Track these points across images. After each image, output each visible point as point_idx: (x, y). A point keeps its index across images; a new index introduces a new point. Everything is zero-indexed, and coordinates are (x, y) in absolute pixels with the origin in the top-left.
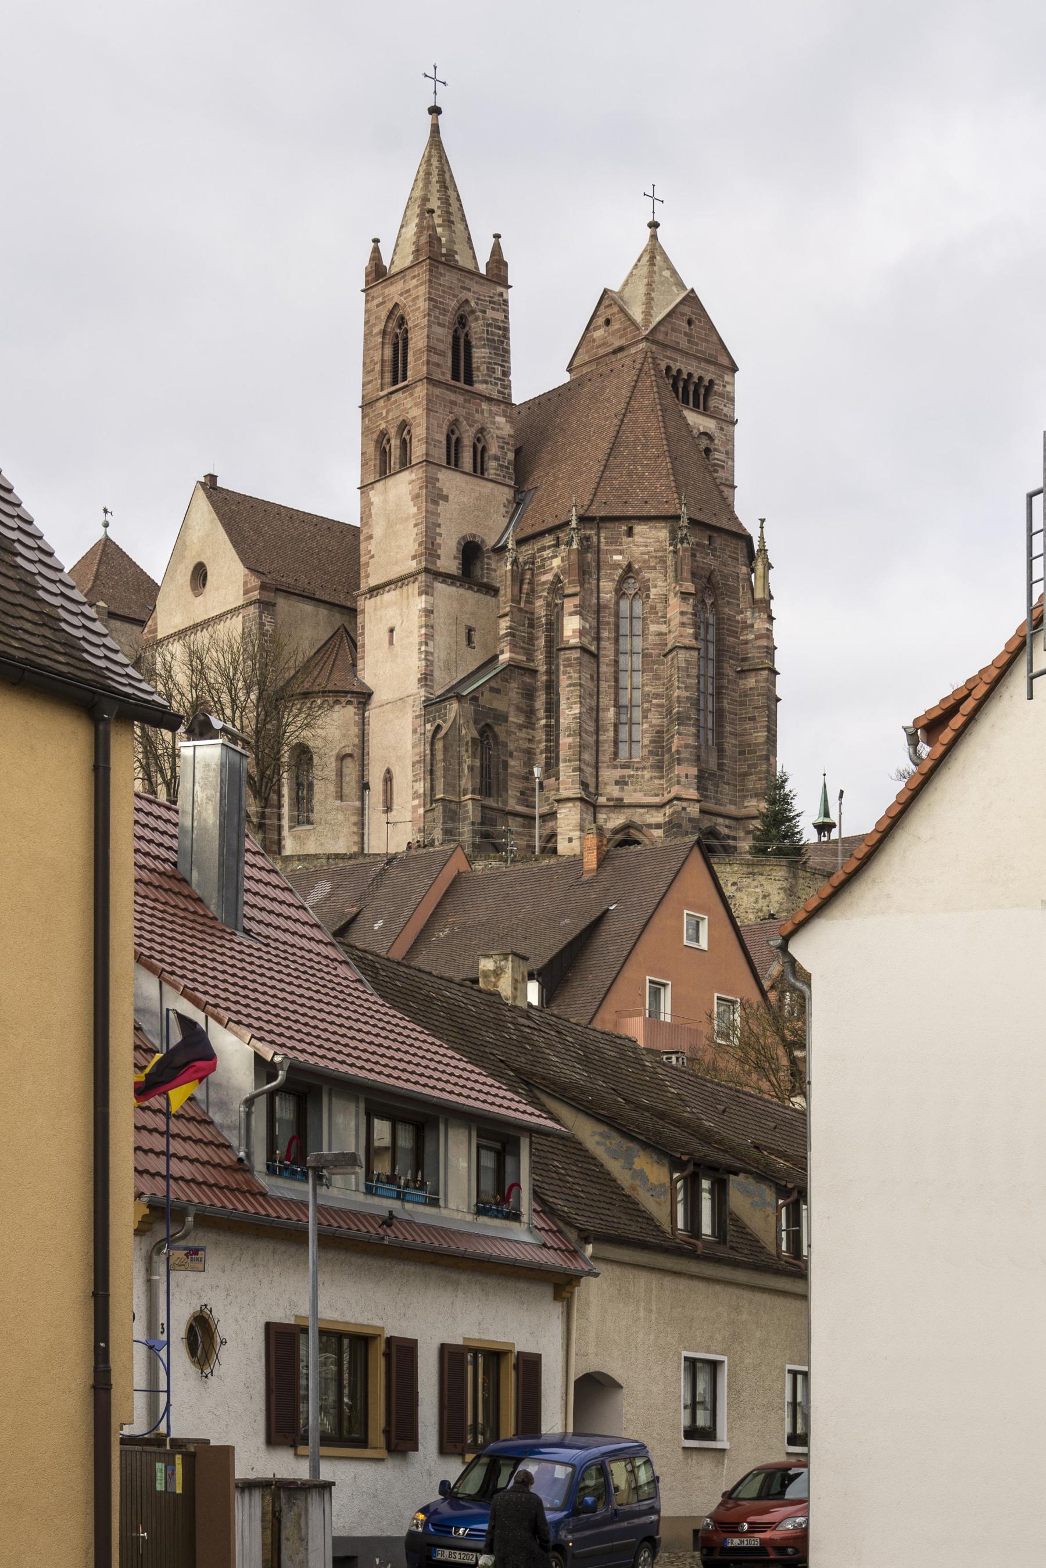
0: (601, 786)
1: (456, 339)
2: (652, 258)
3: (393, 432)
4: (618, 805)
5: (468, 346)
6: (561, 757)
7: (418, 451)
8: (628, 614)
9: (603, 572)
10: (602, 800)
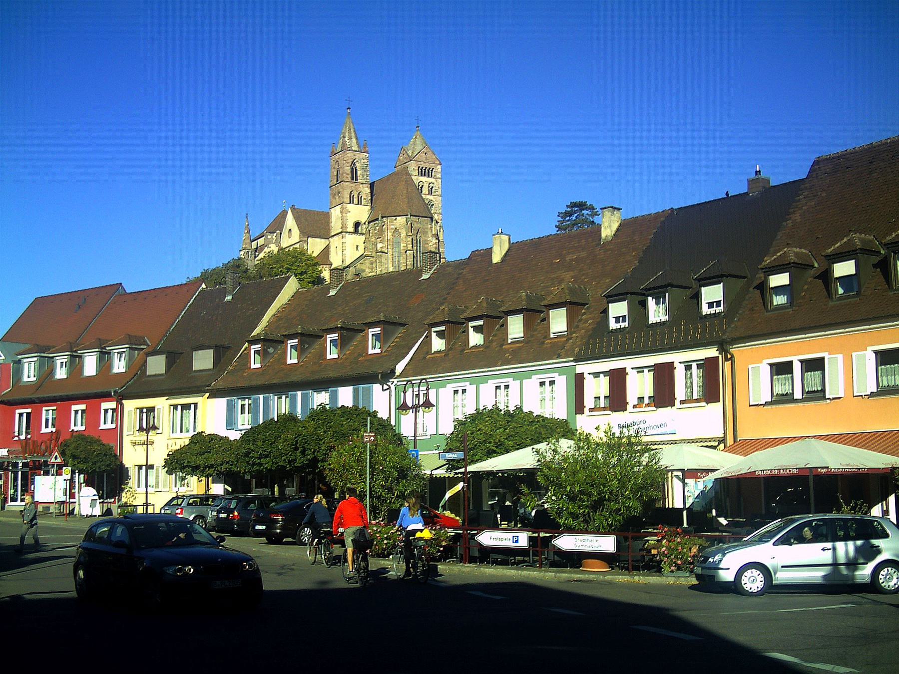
1: (352, 169)
5: (356, 170)
9: (389, 231)
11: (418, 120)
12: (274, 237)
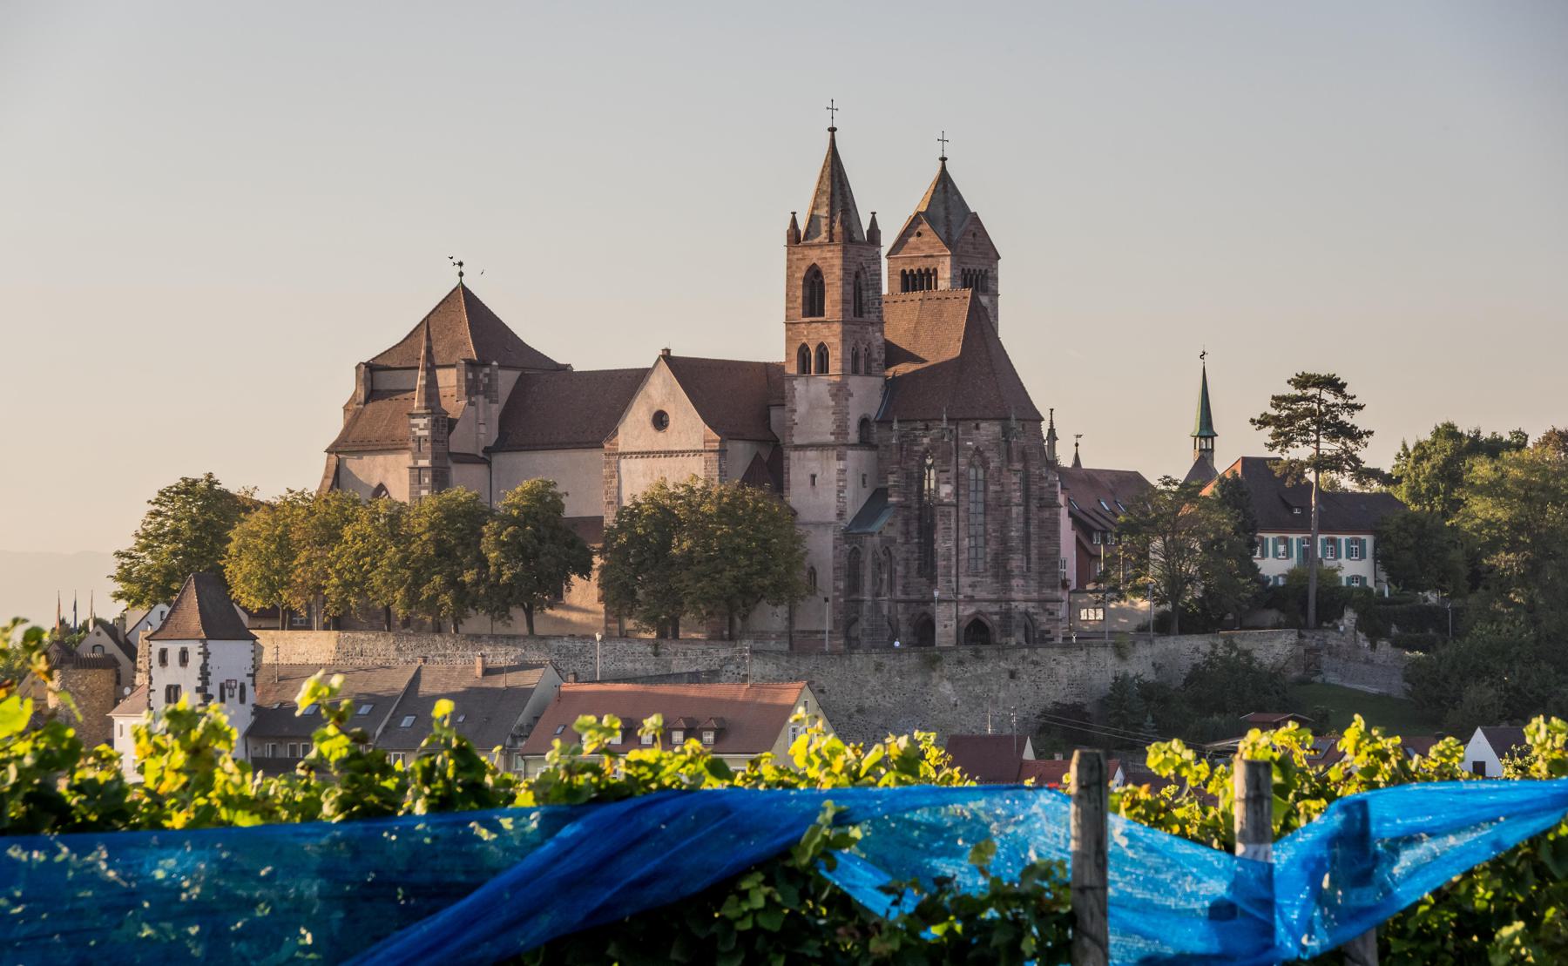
0: (960, 587)
2: (945, 187)
3: (813, 349)
4: (971, 600)
5: (860, 288)
6: (939, 573)
7: (835, 365)
8: (974, 478)
10: (961, 597)
11: (943, 141)
12: (481, 376)
